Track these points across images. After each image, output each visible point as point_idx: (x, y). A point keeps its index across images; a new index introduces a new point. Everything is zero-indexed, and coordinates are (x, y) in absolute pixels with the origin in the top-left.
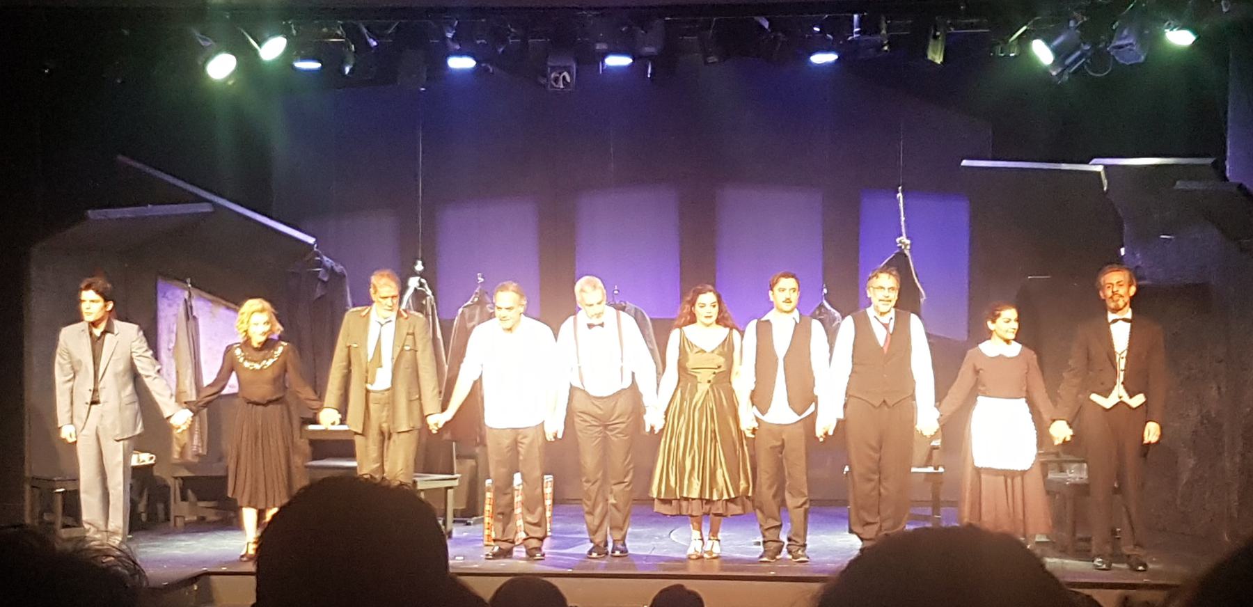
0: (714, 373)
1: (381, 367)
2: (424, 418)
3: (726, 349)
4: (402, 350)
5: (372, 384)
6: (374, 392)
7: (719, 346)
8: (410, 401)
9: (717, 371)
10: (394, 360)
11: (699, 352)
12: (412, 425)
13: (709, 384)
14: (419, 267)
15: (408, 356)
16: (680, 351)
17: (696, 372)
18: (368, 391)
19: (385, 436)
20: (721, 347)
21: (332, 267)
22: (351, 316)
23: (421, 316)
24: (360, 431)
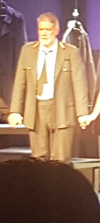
1: (47, 83)
2: (76, 118)
4: (61, 71)
5: (40, 95)
6: (42, 101)
8: (67, 107)
10: (55, 79)
12: (68, 124)
14: (76, 13)
15: (65, 76)
18: (37, 101)
19: (50, 132)
21: (14, 14)
22: (26, 48)
23: (75, 47)
24: (32, 128)
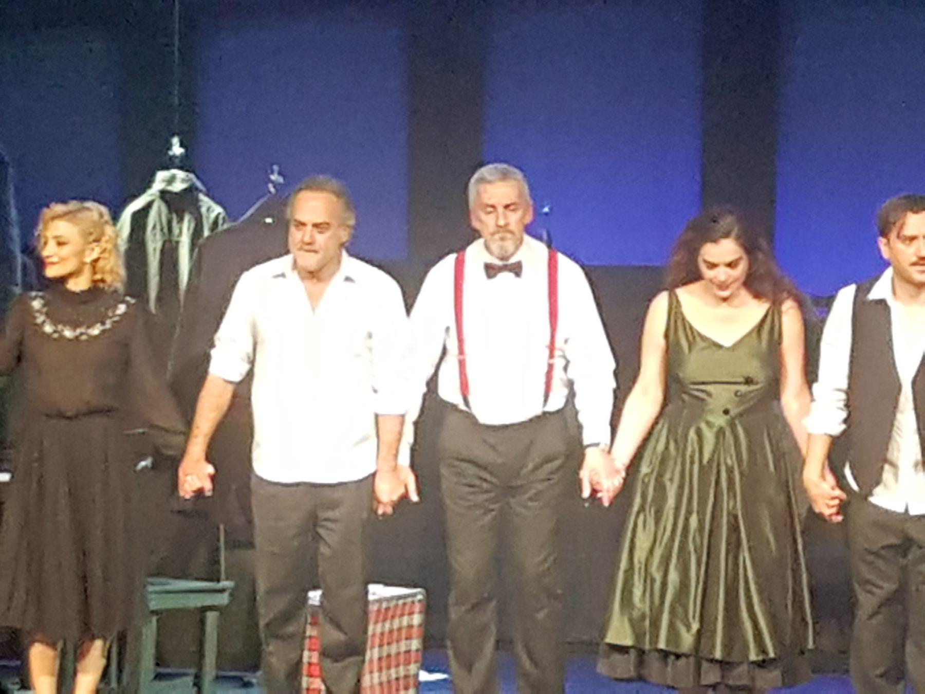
7: (752, 331)
9: (743, 388)
13: (727, 417)
17: (703, 391)
20: (754, 335)
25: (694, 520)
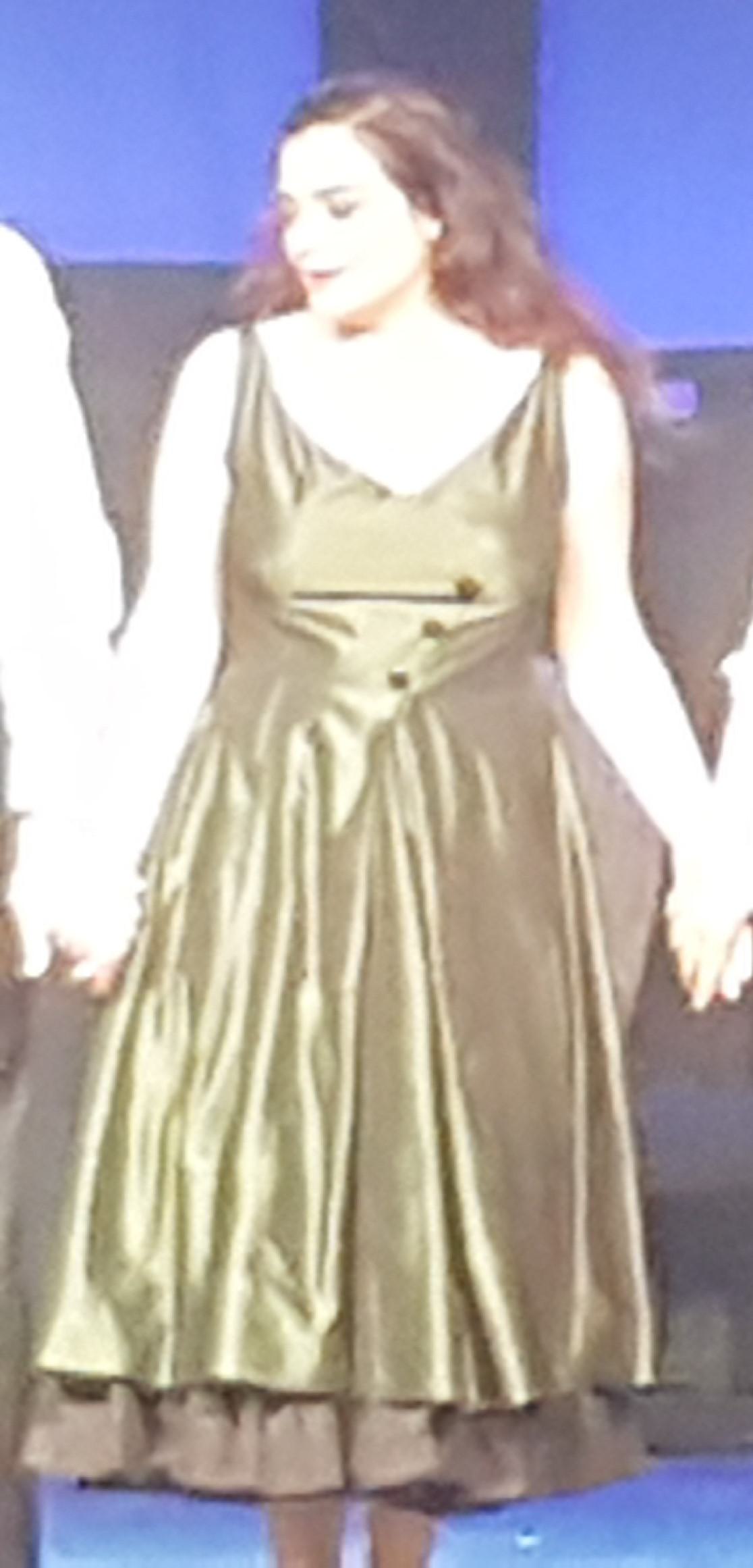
0: (432, 630)
3: (516, 477)
9: (449, 615)
11: (349, 490)
16: (235, 476)
25: (310, 1000)
